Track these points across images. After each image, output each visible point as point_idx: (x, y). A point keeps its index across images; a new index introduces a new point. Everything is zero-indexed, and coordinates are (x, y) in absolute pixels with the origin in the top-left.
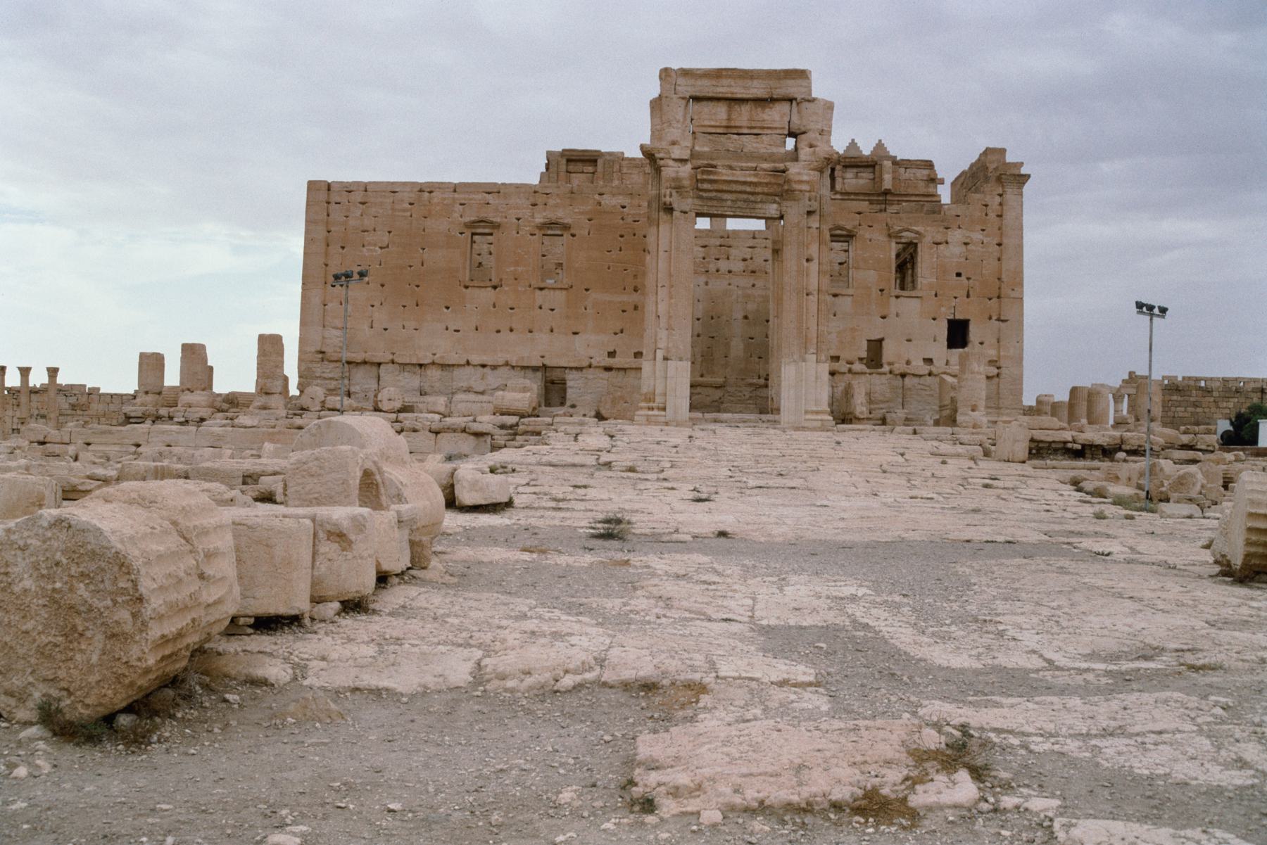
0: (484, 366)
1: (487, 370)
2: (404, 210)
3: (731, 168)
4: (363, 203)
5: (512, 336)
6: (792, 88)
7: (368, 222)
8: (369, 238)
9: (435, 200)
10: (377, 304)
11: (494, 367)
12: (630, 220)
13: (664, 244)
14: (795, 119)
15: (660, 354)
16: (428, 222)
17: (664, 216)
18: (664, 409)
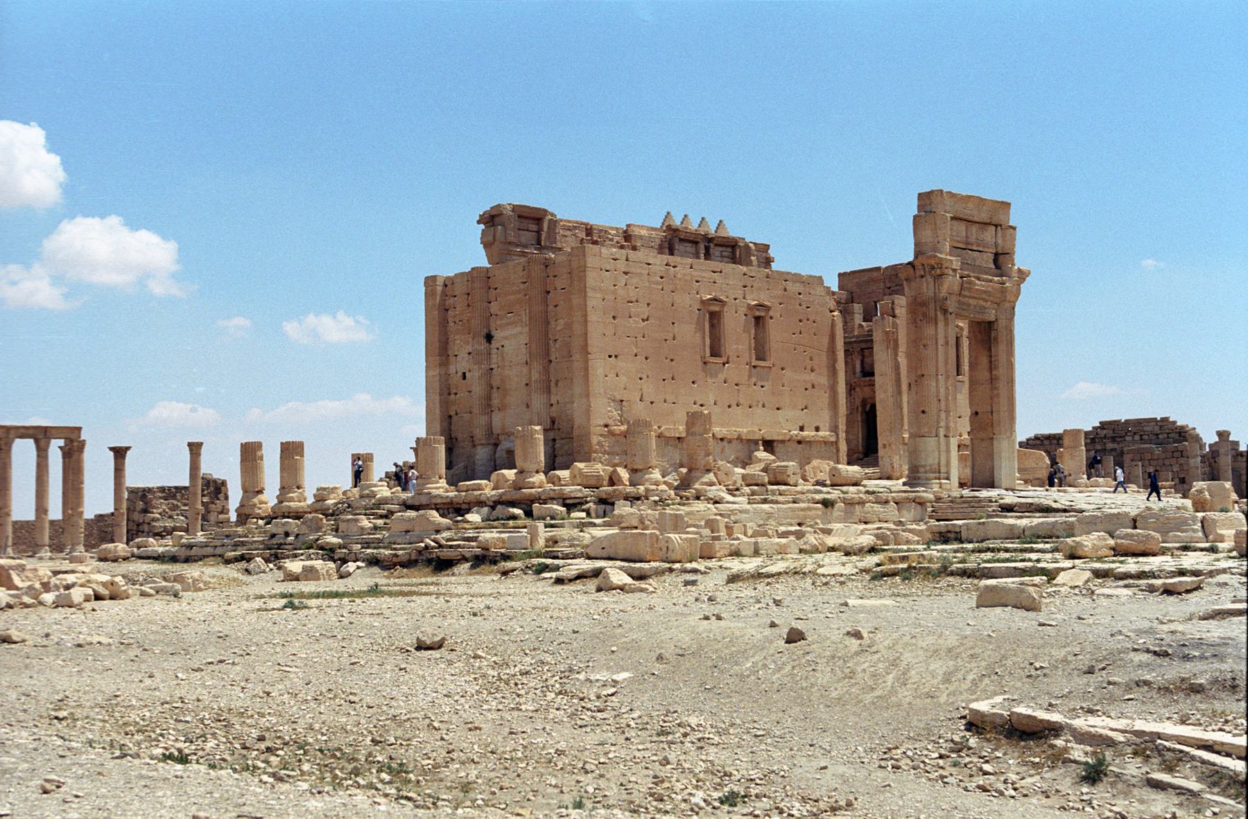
0: (722, 439)
1: (725, 443)
2: (657, 283)
3: (979, 279)
4: (626, 273)
5: (739, 410)
6: (999, 218)
7: (633, 294)
8: (633, 308)
9: (679, 276)
10: (644, 376)
11: (730, 441)
12: (804, 307)
13: (941, 341)
14: (1000, 241)
15: (942, 432)
16: (680, 299)
17: (940, 316)
18: (948, 479)
